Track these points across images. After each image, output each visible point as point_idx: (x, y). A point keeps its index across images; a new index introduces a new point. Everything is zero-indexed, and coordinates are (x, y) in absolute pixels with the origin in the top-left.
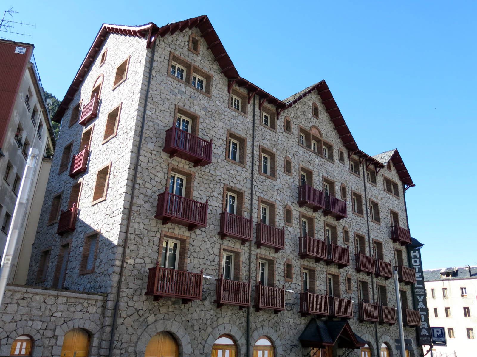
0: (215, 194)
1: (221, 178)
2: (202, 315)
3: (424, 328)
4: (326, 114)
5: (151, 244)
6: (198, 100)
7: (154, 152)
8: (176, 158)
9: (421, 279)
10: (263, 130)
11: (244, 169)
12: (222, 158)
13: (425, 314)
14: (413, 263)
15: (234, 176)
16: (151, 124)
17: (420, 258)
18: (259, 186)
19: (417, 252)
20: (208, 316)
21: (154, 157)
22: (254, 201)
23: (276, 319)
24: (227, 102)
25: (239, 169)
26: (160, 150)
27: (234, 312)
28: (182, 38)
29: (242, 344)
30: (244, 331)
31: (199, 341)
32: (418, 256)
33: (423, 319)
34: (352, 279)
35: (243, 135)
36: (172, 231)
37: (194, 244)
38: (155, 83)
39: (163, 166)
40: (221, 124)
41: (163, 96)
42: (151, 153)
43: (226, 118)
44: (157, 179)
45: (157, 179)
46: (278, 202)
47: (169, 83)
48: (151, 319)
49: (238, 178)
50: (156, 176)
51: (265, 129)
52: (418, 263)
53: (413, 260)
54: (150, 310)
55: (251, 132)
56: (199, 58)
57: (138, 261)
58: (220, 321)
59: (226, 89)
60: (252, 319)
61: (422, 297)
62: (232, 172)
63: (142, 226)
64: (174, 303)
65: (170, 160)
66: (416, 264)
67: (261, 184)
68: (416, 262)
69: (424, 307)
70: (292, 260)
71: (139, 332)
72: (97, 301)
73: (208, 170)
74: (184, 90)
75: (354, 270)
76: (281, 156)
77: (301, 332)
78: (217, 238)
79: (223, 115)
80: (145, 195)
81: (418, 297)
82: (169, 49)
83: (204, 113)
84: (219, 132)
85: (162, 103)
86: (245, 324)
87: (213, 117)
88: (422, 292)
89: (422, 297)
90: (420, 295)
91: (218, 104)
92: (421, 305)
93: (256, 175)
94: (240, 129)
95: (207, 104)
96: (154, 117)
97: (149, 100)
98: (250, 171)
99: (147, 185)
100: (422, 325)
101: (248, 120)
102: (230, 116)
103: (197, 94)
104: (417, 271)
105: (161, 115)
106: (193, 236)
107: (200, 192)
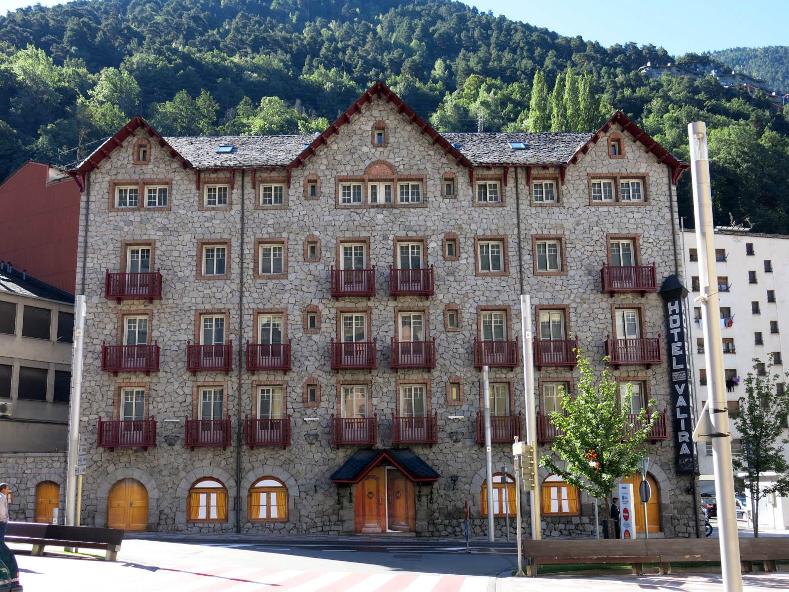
0: (184, 326)
1: (190, 304)
2: (173, 460)
3: (684, 442)
4: (409, 128)
5: (105, 399)
6: (152, 221)
7: (100, 305)
8: (125, 302)
9: (681, 353)
10: (262, 216)
11: (228, 282)
12: (191, 279)
13: (686, 416)
14: (672, 325)
15: (211, 295)
16: (93, 276)
17: (680, 314)
18: (255, 295)
19: (677, 302)
20: (180, 460)
21: (100, 310)
22: (246, 317)
23: (287, 455)
24: (196, 204)
25: (220, 283)
26: (105, 300)
27: (218, 453)
28: (125, 155)
29: (231, 487)
30: (233, 473)
31: (170, 485)
32: (677, 311)
33: (683, 427)
35: (226, 236)
36: (128, 380)
37: (157, 388)
38: (94, 227)
39: (112, 315)
40: (187, 237)
41: (105, 239)
42: (97, 307)
43: (195, 225)
44: (105, 332)
45: (105, 332)
46: (290, 307)
47: (111, 219)
48: (111, 468)
49: (218, 295)
50: (105, 328)
51: (265, 212)
52: (678, 324)
53: (671, 318)
54: (109, 461)
55: (239, 226)
56: (151, 166)
57: (92, 417)
58: (197, 464)
59: (194, 187)
60: (245, 458)
61: (683, 385)
62: (207, 291)
63: (93, 383)
64: (136, 451)
65: (120, 307)
66: (675, 325)
67: (259, 291)
68: (675, 321)
70: (320, 379)
71: (99, 480)
72: (59, 457)
73: (171, 301)
74: (132, 218)
75: (472, 369)
76: (298, 239)
77: (336, 469)
78: (187, 376)
79: (190, 225)
80: (94, 353)
81: (677, 386)
82: (108, 178)
83: (161, 234)
84: (186, 249)
85: (105, 247)
86: (234, 465)
87: (175, 234)
88: (683, 378)
89: (683, 385)
90: (680, 383)
91: (182, 212)
92: (681, 402)
93: (250, 282)
94: (220, 230)
95: (165, 221)
96: (97, 266)
97: (89, 250)
98: (238, 281)
99: (95, 341)
101: (232, 212)
102: (202, 219)
103: (149, 214)
104: (676, 339)
105: (105, 260)
106: (155, 380)
107: (161, 330)
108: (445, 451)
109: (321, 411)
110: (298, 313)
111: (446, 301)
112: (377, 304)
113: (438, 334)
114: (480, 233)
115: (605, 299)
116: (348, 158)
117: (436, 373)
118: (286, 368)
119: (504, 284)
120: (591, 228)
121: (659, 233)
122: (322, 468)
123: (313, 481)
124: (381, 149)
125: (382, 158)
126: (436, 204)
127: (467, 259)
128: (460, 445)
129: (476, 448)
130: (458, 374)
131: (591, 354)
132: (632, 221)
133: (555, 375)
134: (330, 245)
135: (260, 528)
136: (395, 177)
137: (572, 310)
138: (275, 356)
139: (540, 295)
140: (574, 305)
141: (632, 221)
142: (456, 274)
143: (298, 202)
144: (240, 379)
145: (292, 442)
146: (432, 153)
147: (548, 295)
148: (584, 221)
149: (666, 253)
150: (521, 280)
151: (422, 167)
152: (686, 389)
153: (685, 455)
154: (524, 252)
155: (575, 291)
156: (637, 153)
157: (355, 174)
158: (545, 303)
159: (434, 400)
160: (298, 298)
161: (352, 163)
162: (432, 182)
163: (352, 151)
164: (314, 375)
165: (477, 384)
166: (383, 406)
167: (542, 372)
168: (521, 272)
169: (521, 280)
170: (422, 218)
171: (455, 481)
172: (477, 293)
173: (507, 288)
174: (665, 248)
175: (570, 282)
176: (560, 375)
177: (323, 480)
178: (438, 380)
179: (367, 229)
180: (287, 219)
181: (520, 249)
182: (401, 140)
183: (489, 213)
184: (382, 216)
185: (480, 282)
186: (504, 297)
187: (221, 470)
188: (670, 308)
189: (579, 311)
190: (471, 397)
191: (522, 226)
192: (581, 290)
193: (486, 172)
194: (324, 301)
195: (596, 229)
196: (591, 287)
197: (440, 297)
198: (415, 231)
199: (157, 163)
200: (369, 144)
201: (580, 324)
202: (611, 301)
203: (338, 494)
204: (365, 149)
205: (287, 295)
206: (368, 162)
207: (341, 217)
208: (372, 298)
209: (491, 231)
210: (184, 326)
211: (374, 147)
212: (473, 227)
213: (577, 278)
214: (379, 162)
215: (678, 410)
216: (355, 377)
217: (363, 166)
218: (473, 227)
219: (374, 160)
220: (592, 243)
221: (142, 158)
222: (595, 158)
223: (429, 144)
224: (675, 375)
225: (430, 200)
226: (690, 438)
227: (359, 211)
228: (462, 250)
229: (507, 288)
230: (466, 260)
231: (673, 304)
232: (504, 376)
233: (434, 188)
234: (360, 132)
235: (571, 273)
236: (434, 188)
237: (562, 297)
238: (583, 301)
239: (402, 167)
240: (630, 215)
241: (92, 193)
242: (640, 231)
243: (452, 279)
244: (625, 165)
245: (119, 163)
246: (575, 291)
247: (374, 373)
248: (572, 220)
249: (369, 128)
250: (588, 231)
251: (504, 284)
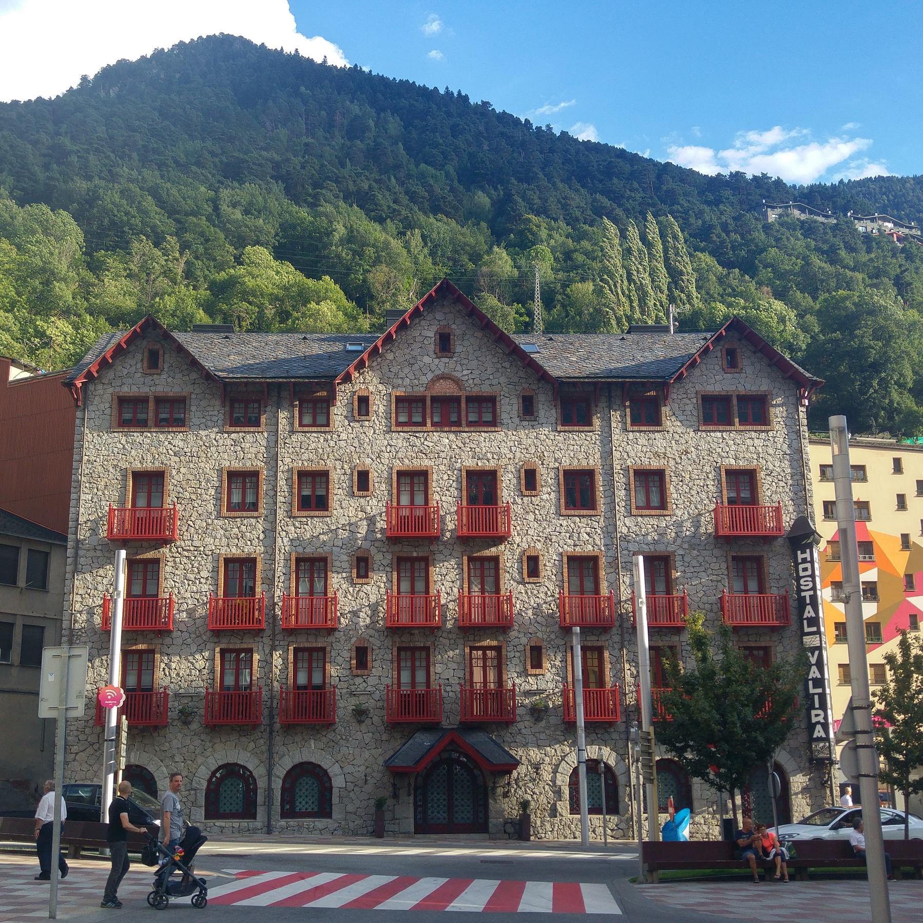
3: (819, 723)
7: (99, 548)
13: (820, 690)
19: (808, 551)
21: (99, 553)
28: (133, 362)
29: (260, 777)
32: (809, 559)
56: (165, 376)
61: (817, 653)
69: (819, 676)
82: (111, 390)
89: (817, 653)
100: (817, 715)
108: (523, 731)
109: (372, 681)
110: (345, 558)
111: (524, 545)
116: (406, 370)
122: (373, 751)
123: (363, 768)
124: (447, 360)
125: (446, 371)
130: (540, 635)
135: (296, 828)
136: (463, 394)
137: (678, 558)
140: (681, 552)
146: (507, 365)
151: (495, 382)
152: (820, 657)
153: (820, 739)
157: (416, 389)
161: (411, 376)
163: (412, 361)
166: (449, 674)
171: (537, 769)
177: (376, 767)
187: (249, 754)
188: (800, 556)
189: (687, 559)
199: (172, 373)
201: (689, 575)
203: (394, 785)
204: (427, 360)
206: (430, 376)
207: (399, 440)
211: (437, 357)
214: (443, 377)
215: (810, 683)
217: (424, 380)
219: (438, 372)
222: (705, 373)
223: (504, 354)
224: (807, 639)
226: (826, 718)
230: (548, 494)
231: (803, 552)
233: (509, 407)
234: (421, 339)
236: (509, 407)
240: (749, 442)
244: (742, 381)
245: (125, 371)
249: (431, 334)
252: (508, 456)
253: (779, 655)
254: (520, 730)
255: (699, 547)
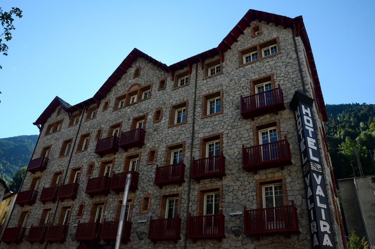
34: (150, 198)
49: (63, 164)
55: (77, 131)
70: (86, 201)
83: (54, 141)
111: (151, 147)
112: (119, 155)
113: (143, 167)
114: (174, 103)
115: (249, 123)
117: (138, 192)
118: (74, 198)
119: (183, 129)
120: (239, 80)
121: (288, 68)
126: (155, 95)
127: (165, 120)
128: (143, 242)
129: (152, 244)
130: (149, 192)
131: (237, 165)
132: (268, 67)
133: (210, 185)
134: (106, 130)
138: (71, 191)
139: (205, 130)
141: (268, 67)
142: (158, 130)
143: (100, 113)
144: (58, 204)
145: (67, 240)
147: (210, 129)
148: (235, 78)
149: (294, 79)
150: (194, 123)
154: (197, 106)
155: (227, 123)
156: (270, 29)
158: (207, 135)
159: (134, 210)
160: (88, 159)
162: (155, 85)
164: (84, 200)
165: (159, 198)
167: (201, 183)
168: (194, 119)
169: (194, 123)
170: (148, 104)
172: (168, 138)
173: (185, 131)
174: (294, 76)
175: (224, 118)
176: (213, 184)
178: (138, 197)
179: (123, 117)
180: (94, 123)
181: (195, 105)
182: (145, 72)
183: (180, 91)
184: (130, 109)
185: (169, 132)
186: (182, 137)
190: (154, 207)
191: (198, 92)
192: (232, 121)
193: (181, 71)
194: (97, 159)
195: (243, 79)
196: (239, 116)
197: (148, 145)
198: (143, 112)
200: (132, 78)
202: (253, 123)
204: (130, 81)
205: (85, 158)
208: (117, 153)
209: (180, 100)
210: (49, 181)
212: (171, 101)
213: (229, 113)
214: (134, 85)
216: (100, 199)
217: (127, 89)
218: (171, 101)
219: (132, 84)
220: (241, 88)
221: (59, 113)
225: (152, 94)
227: (120, 110)
228: (163, 116)
229: (185, 131)
232: (176, 190)
235: (225, 111)
237: (218, 128)
238: (233, 127)
239: (143, 83)
241: (43, 131)
242: (274, 71)
243: (155, 133)
246: (227, 123)
247: (109, 195)
248: (227, 80)
250: (237, 82)
251: (183, 129)
252: (151, 108)
253: (288, 185)
254: (132, 246)
255: (237, 127)
